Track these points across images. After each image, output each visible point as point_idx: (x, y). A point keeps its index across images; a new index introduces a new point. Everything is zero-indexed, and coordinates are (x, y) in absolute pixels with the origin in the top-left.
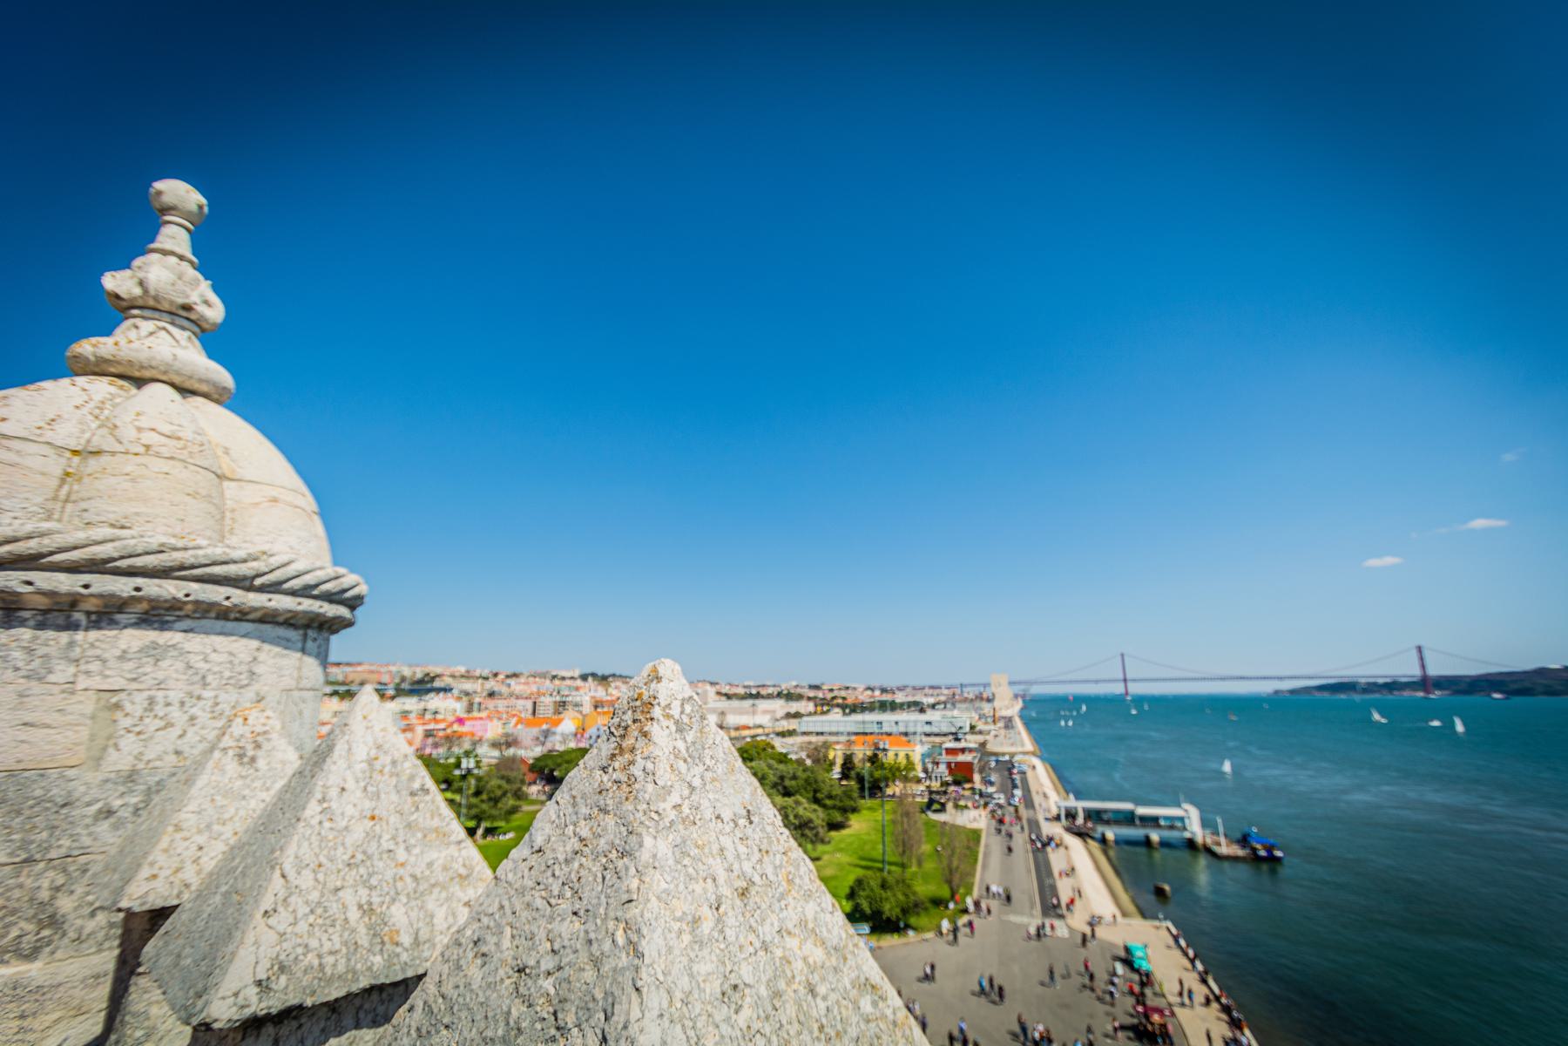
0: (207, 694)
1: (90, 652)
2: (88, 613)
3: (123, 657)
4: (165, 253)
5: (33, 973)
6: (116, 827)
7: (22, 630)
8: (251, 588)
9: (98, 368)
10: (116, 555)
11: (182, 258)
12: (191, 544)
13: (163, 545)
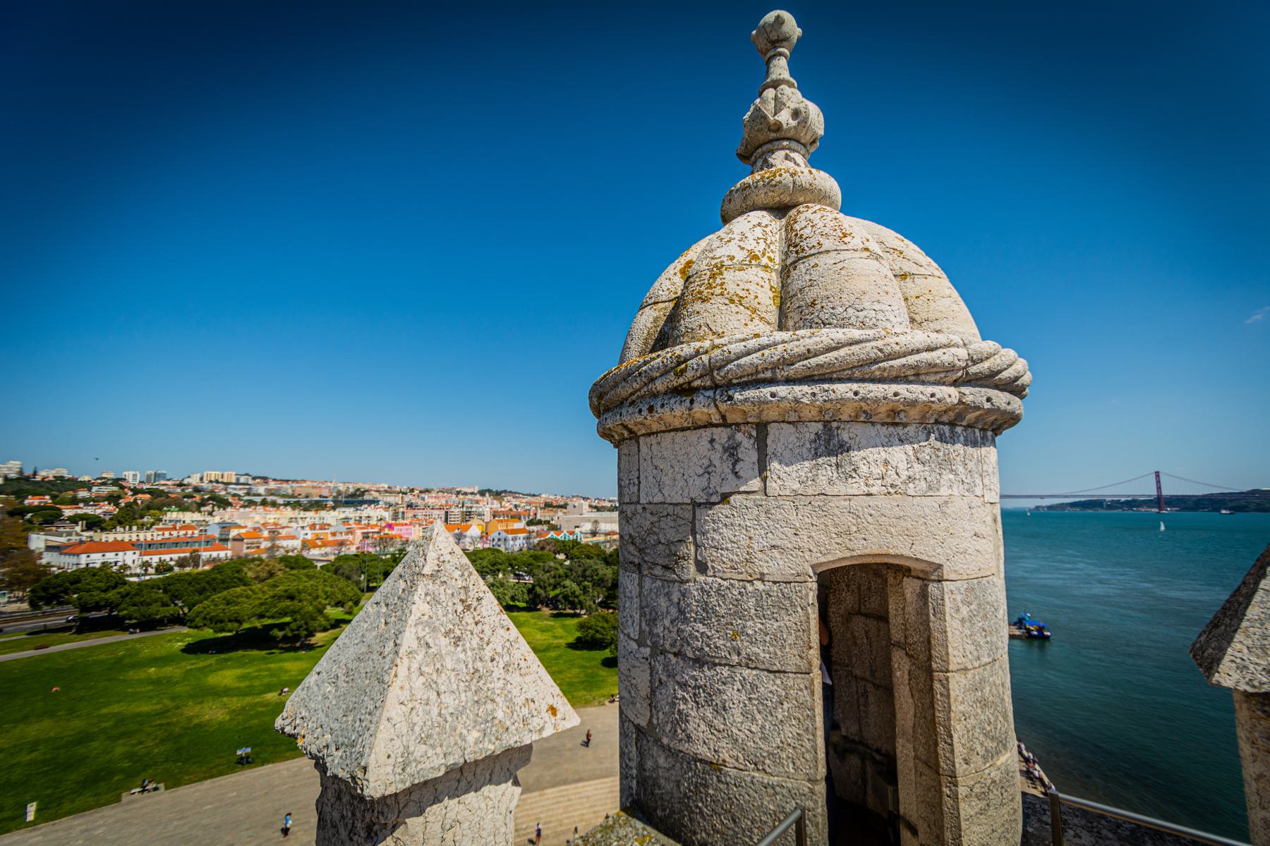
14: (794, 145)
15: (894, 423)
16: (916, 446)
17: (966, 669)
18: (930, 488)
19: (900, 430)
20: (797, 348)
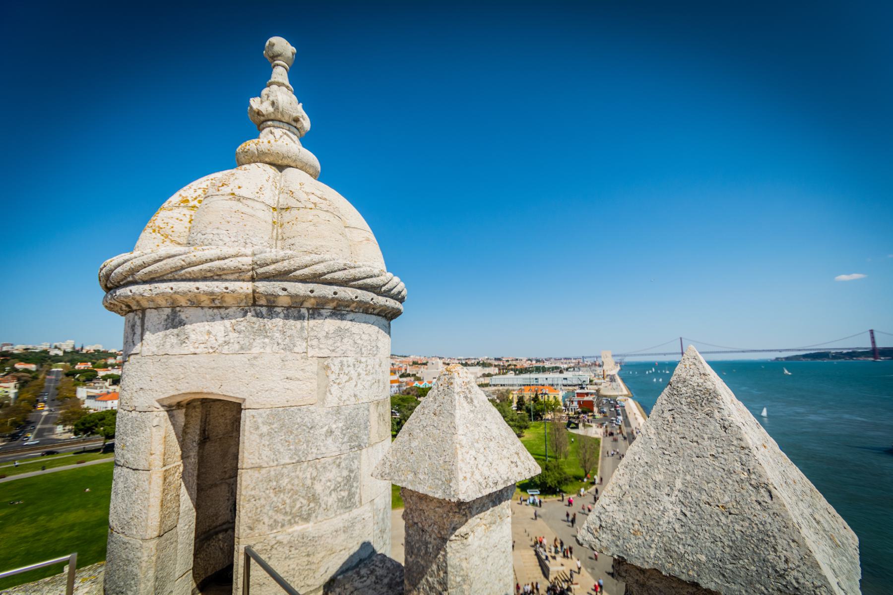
0: (363, 360)
1: (312, 334)
2: (308, 309)
3: (327, 337)
4: (280, 84)
5: (310, 529)
6: (335, 441)
7: (278, 319)
8: (380, 294)
9: (260, 158)
10: (325, 271)
11: (287, 87)
13: (345, 265)
14: (276, 124)
15: (217, 306)
16: (233, 321)
17: (261, 467)
18: (242, 348)
19: (222, 311)
20: (191, 258)
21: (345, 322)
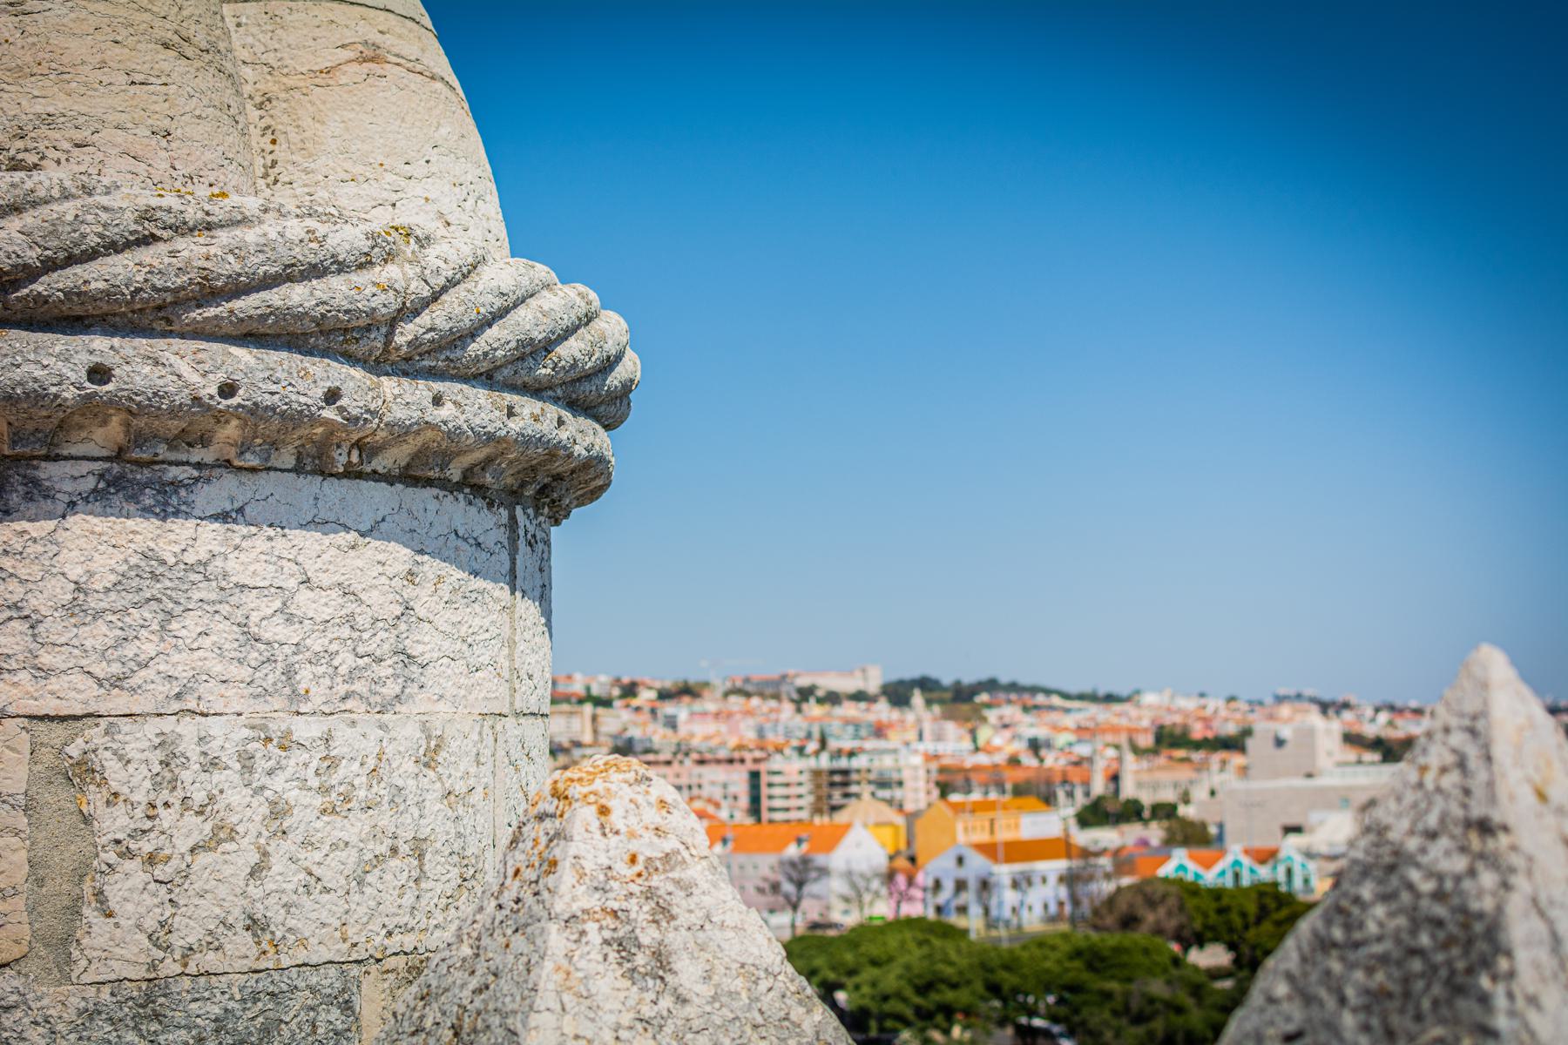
0: (307, 730)
8: (379, 365)
10: (32, 256)
12: (219, 212)
13: (146, 215)
21: (182, 529)
